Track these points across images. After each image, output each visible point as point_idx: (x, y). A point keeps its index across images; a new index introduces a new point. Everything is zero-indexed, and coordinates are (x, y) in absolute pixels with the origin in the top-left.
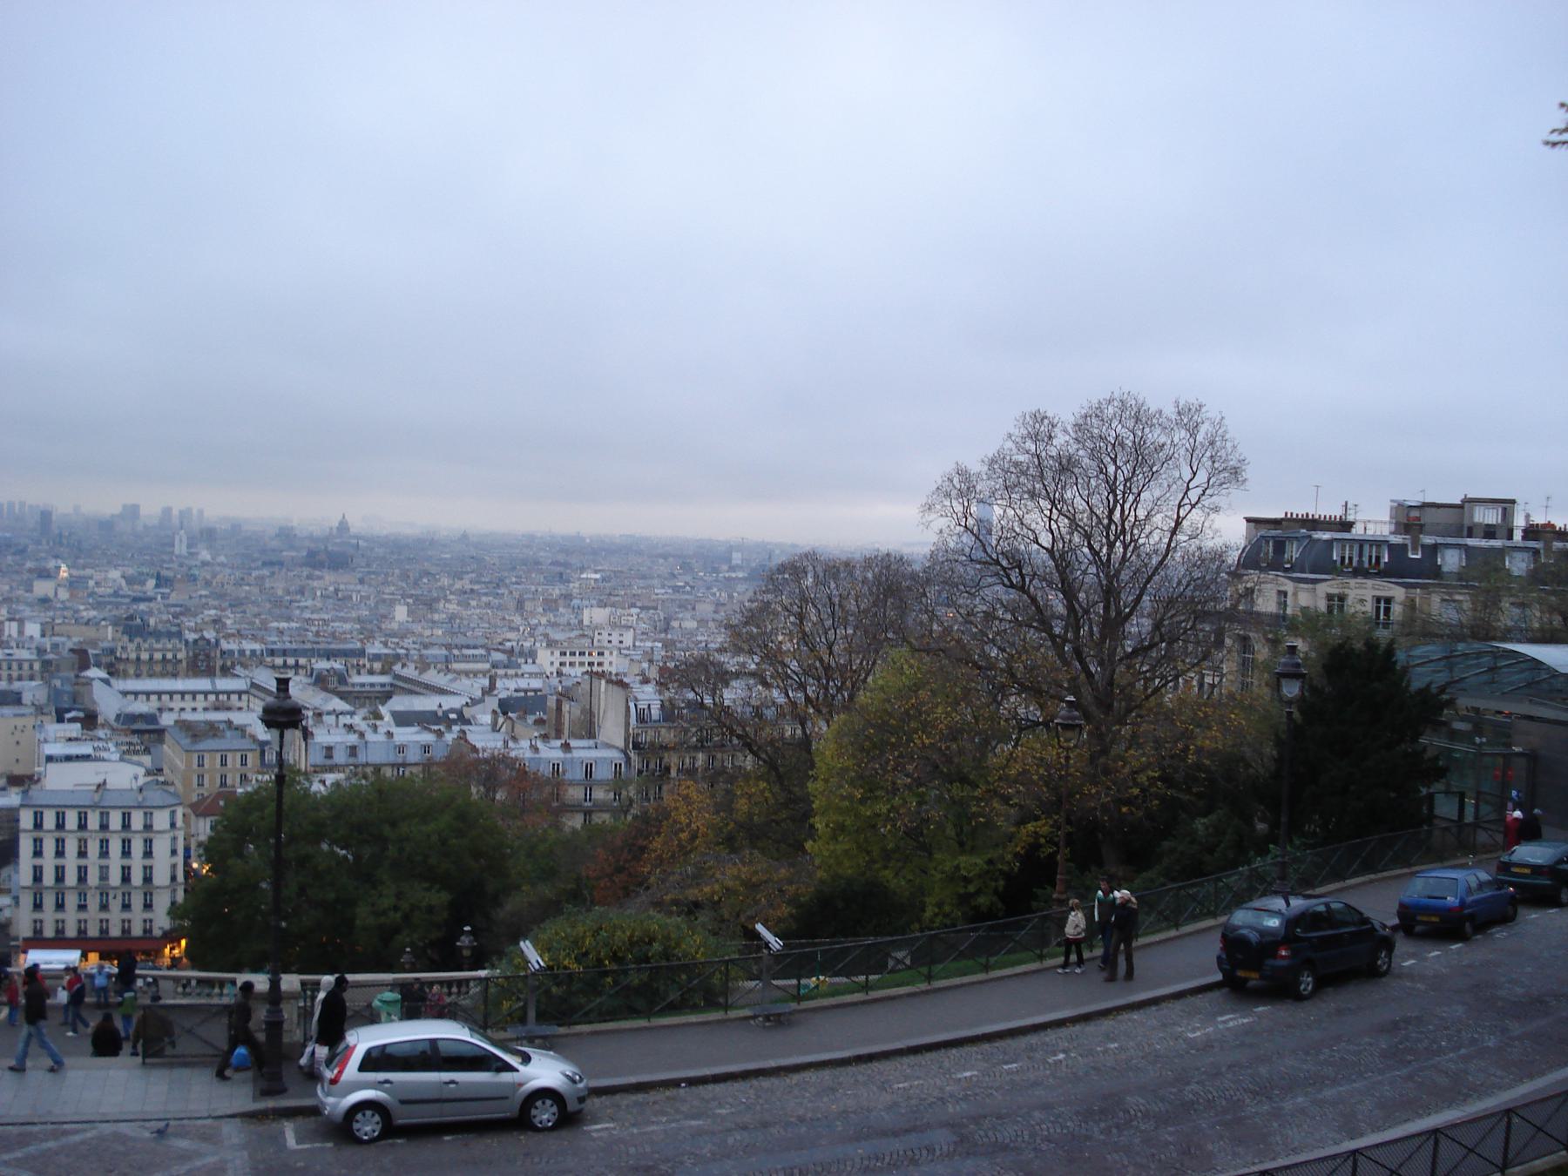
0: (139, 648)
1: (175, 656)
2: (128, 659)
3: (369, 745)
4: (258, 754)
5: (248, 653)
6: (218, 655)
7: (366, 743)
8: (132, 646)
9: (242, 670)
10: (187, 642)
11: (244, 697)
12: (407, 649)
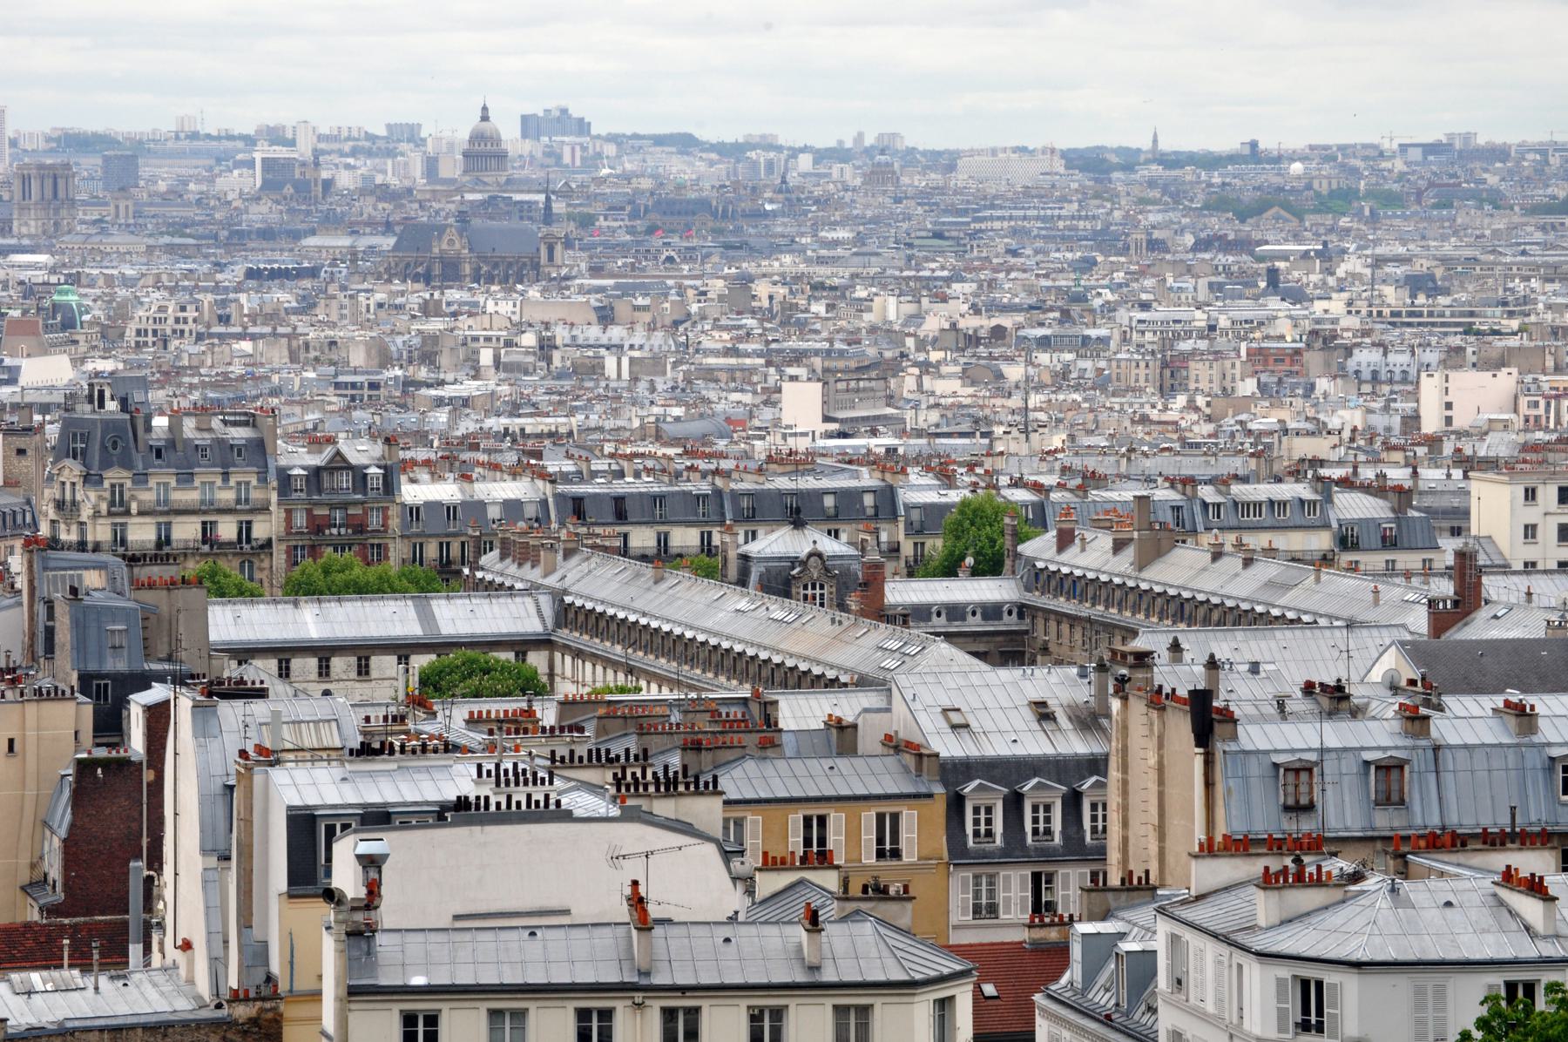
0: (119, 507)
1: (245, 529)
2: (81, 546)
3: (1447, 757)
4: (939, 808)
5: (494, 512)
6: (394, 523)
7: (1437, 749)
8: (89, 500)
9: (513, 569)
10: (285, 479)
11: (537, 660)
12: (1037, 487)
